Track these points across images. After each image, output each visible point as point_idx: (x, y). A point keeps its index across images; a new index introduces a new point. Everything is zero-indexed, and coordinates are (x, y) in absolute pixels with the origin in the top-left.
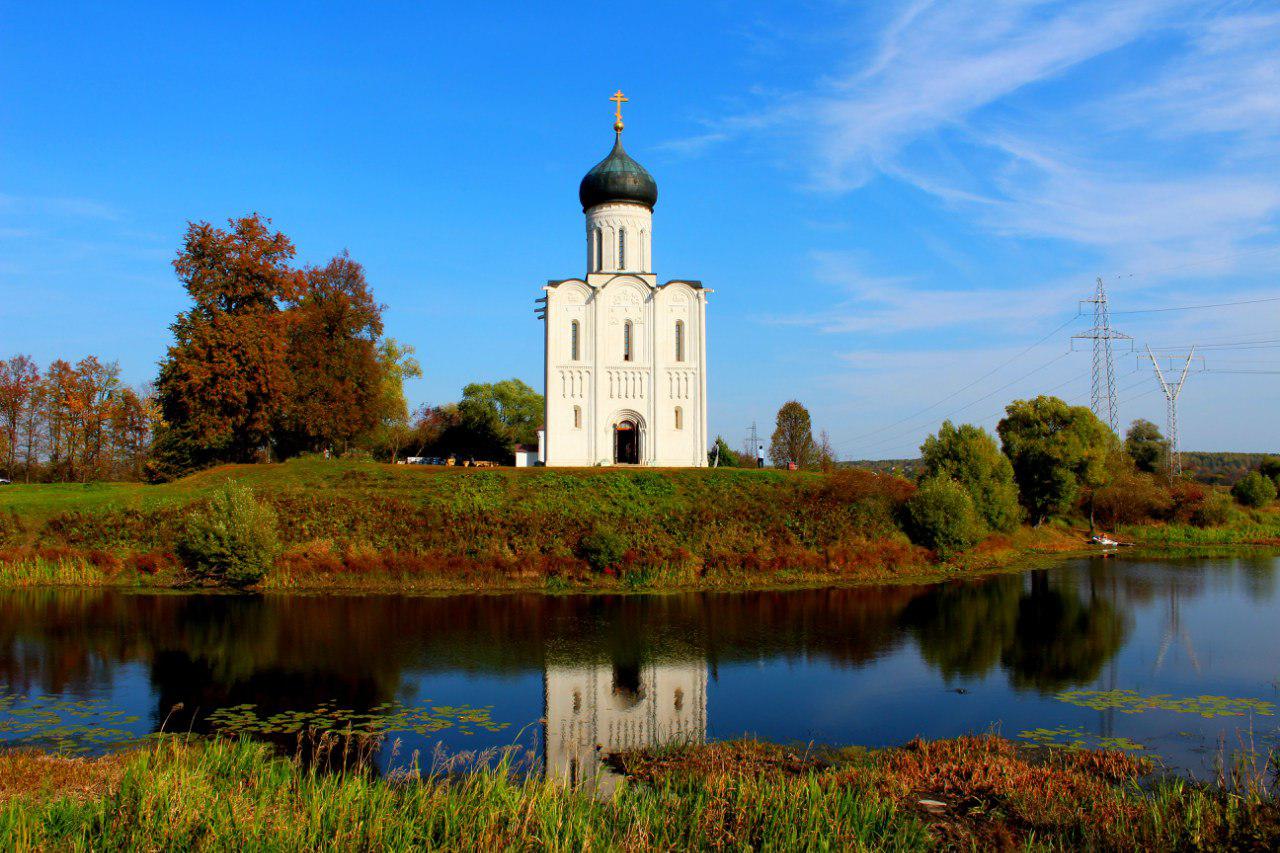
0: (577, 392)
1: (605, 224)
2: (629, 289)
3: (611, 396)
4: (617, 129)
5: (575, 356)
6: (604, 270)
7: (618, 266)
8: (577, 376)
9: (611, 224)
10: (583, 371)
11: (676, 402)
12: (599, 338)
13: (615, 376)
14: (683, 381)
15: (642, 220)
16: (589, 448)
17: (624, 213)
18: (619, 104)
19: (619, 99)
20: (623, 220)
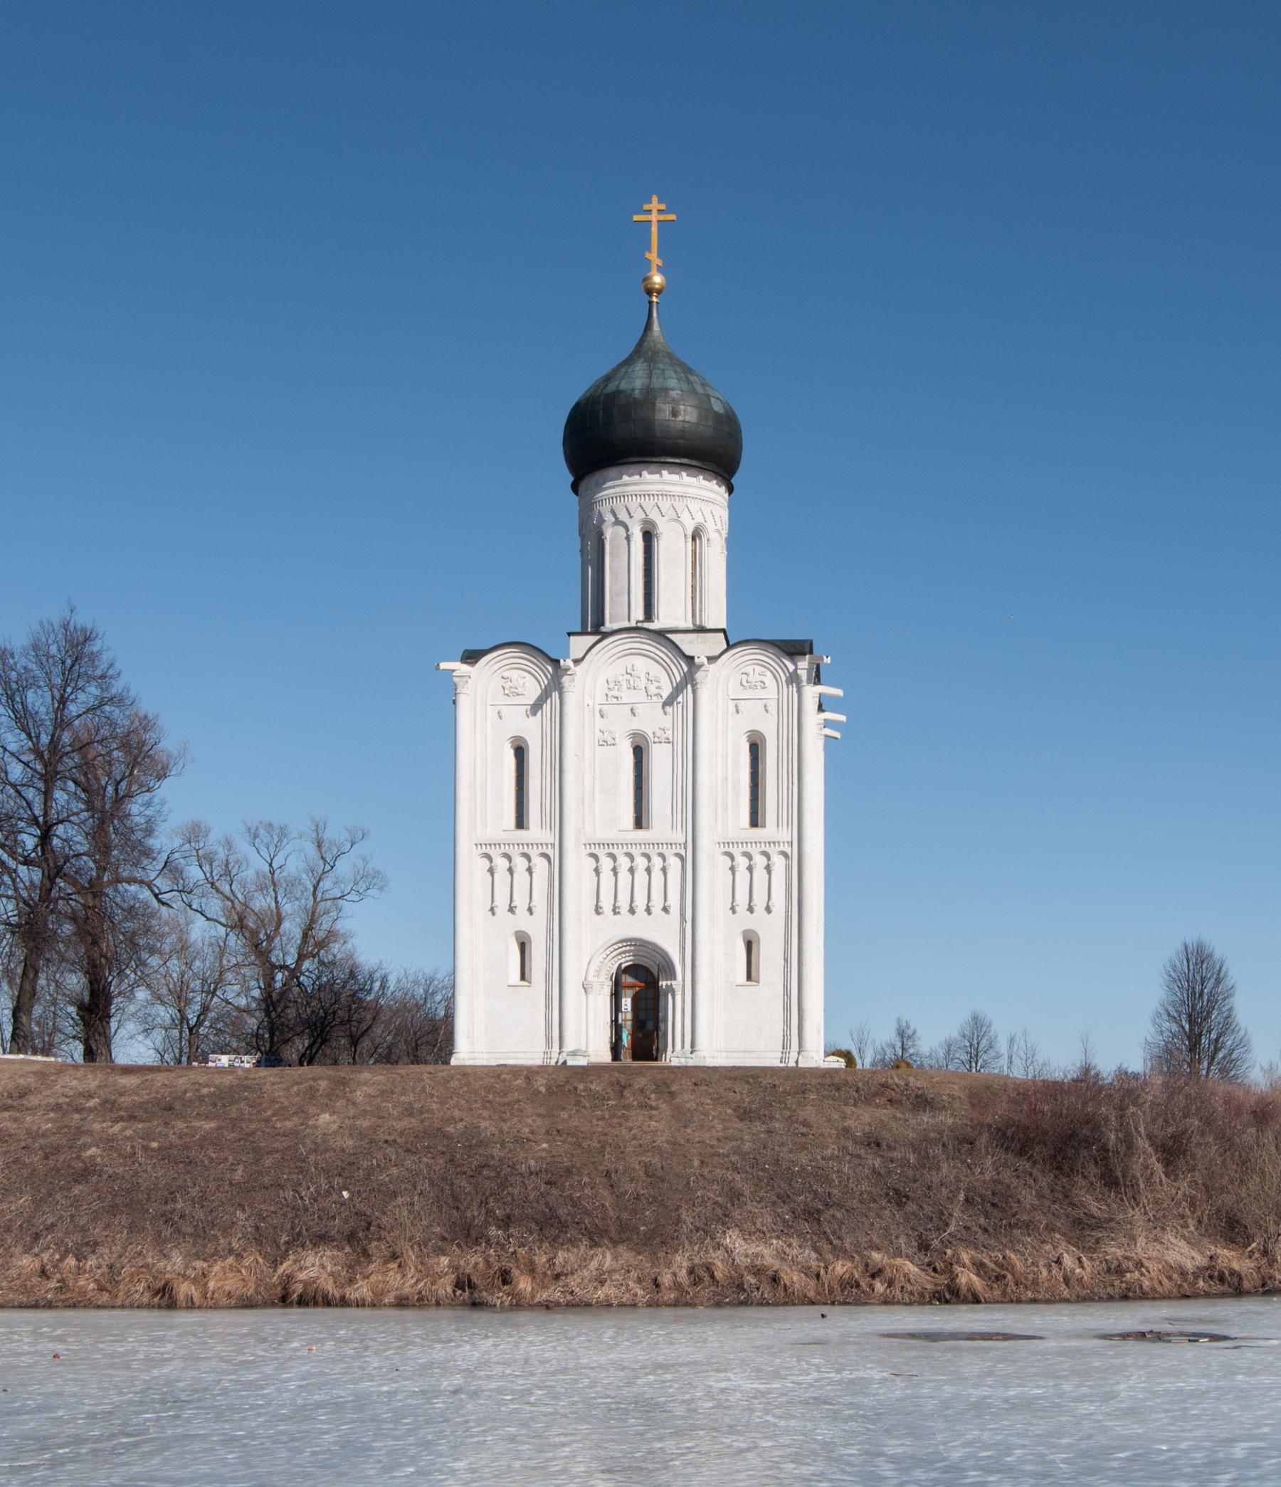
0: (521, 902)
1: (609, 518)
2: (642, 665)
3: (598, 910)
5: (521, 823)
6: (609, 625)
7: (638, 613)
9: (623, 516)
10: (534, 853)
12: (569, 778)
13: (606, 864)
15: (707, 509)
17: (653, 488)
18: (654, 229)
19: (654, 217)
20: (648, 504)
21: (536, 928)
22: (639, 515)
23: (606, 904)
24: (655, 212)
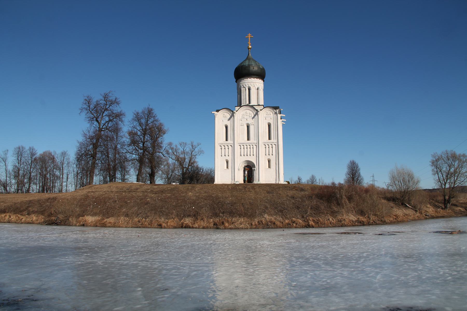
0: (227, 154)
1: (242, 86)
2: (248, 111)
3: (241, 155)
4: (249, 49)
5: (227, 140)
7: (247, 103)
8: (227, 147)
9: (245, 86)
10: (229, 145)
11: (268, 157)
12: (235, 132)
13: (242, 147)
14: (270, 148)
16: (232, 177)
20: (249, 84)
21: (230, 159)
22: (247, 86)
23: (242, 154)
24: (249, 36)
